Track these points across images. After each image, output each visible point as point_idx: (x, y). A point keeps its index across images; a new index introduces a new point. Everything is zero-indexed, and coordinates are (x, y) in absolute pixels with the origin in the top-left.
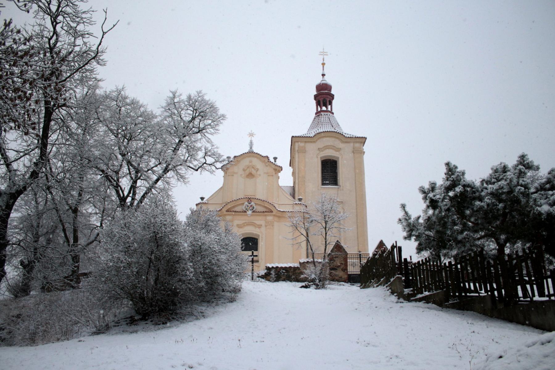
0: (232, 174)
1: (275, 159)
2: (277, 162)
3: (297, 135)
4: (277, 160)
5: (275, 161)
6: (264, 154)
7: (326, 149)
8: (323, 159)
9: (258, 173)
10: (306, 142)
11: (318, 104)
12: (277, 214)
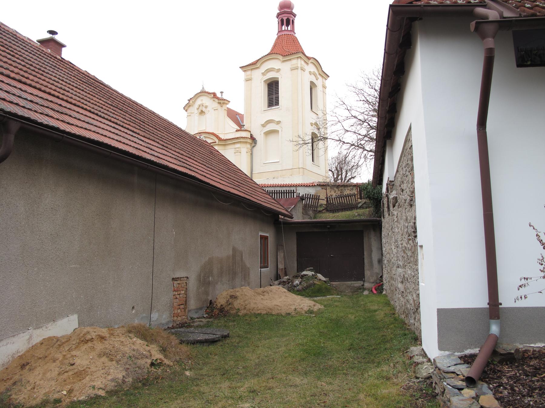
0: (190, 114)
1: (222, 92)
2: (223, 96)
3: (244, 65)
4: (223, 94)
5: (222, 95)
6: (211, 92)
7: (268, 72)
8: (268, 82)
9: (209, 109)
10: (252, 69)
11: (282, 23)
12: (219, 143)
